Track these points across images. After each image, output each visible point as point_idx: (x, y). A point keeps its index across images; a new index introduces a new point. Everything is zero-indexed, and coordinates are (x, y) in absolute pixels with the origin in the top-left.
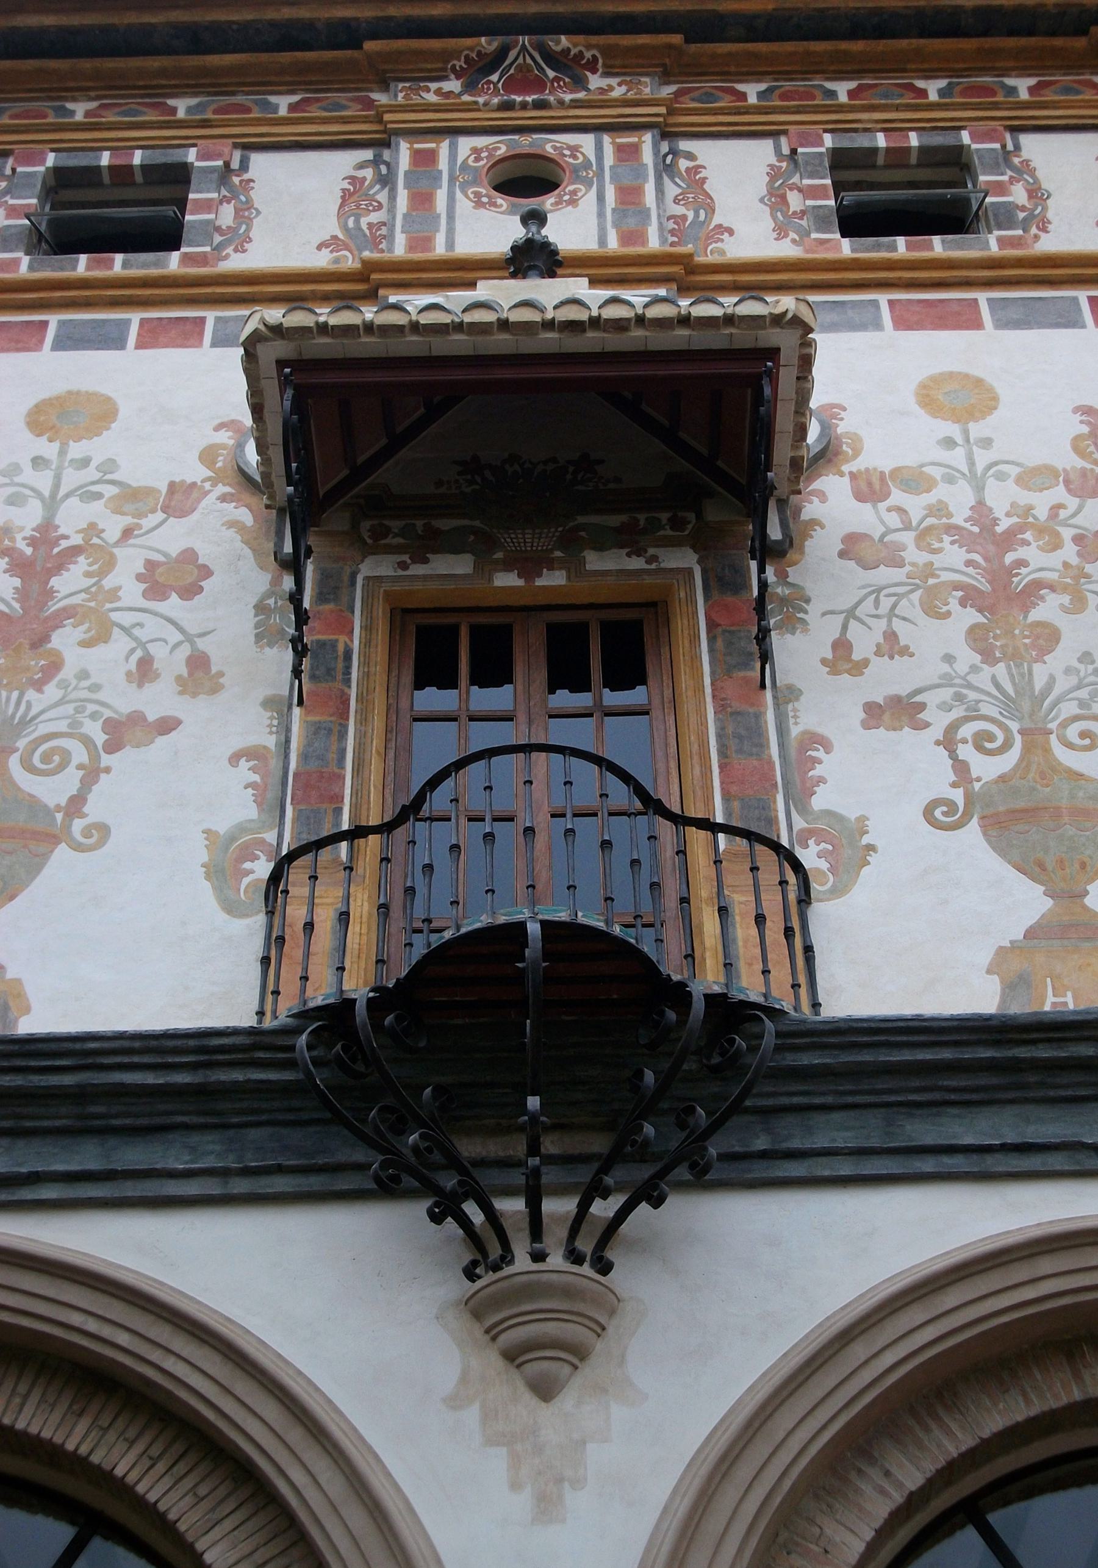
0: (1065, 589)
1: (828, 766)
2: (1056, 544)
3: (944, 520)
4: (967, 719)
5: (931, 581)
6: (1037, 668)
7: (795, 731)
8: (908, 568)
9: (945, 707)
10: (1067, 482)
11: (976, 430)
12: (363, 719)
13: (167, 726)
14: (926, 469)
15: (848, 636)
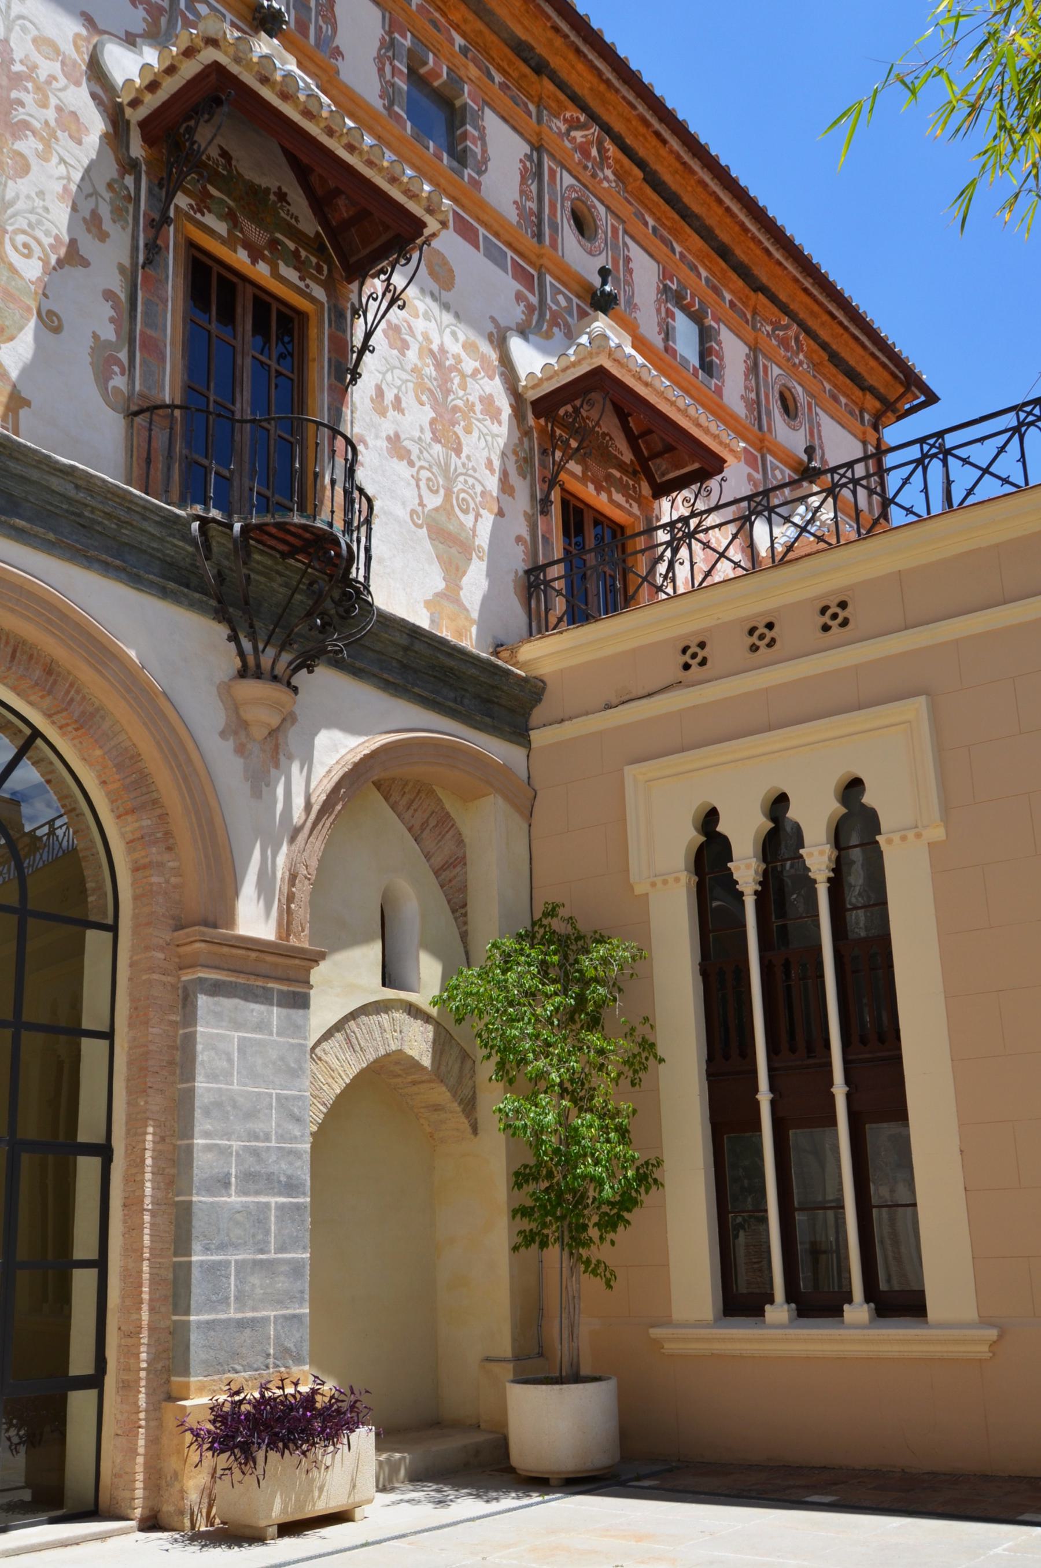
0: (42, 139)
2: (44, 104)
6: (10, 183)
10: (63, 63)
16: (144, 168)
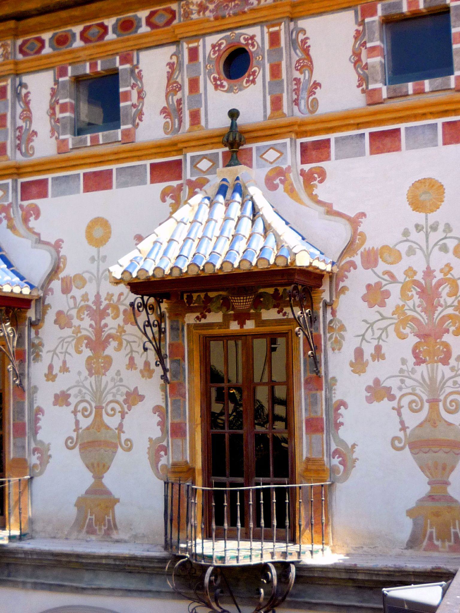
1: (43, 422)
2: (116, 317)
3: (86, 303)
5: (79, 335)
6: (104, 377)
7: (35, 406)
8: (73, 328)
9: (76, 396)
11: (104, 250)
15: (53, 363)
16: (167, 315)
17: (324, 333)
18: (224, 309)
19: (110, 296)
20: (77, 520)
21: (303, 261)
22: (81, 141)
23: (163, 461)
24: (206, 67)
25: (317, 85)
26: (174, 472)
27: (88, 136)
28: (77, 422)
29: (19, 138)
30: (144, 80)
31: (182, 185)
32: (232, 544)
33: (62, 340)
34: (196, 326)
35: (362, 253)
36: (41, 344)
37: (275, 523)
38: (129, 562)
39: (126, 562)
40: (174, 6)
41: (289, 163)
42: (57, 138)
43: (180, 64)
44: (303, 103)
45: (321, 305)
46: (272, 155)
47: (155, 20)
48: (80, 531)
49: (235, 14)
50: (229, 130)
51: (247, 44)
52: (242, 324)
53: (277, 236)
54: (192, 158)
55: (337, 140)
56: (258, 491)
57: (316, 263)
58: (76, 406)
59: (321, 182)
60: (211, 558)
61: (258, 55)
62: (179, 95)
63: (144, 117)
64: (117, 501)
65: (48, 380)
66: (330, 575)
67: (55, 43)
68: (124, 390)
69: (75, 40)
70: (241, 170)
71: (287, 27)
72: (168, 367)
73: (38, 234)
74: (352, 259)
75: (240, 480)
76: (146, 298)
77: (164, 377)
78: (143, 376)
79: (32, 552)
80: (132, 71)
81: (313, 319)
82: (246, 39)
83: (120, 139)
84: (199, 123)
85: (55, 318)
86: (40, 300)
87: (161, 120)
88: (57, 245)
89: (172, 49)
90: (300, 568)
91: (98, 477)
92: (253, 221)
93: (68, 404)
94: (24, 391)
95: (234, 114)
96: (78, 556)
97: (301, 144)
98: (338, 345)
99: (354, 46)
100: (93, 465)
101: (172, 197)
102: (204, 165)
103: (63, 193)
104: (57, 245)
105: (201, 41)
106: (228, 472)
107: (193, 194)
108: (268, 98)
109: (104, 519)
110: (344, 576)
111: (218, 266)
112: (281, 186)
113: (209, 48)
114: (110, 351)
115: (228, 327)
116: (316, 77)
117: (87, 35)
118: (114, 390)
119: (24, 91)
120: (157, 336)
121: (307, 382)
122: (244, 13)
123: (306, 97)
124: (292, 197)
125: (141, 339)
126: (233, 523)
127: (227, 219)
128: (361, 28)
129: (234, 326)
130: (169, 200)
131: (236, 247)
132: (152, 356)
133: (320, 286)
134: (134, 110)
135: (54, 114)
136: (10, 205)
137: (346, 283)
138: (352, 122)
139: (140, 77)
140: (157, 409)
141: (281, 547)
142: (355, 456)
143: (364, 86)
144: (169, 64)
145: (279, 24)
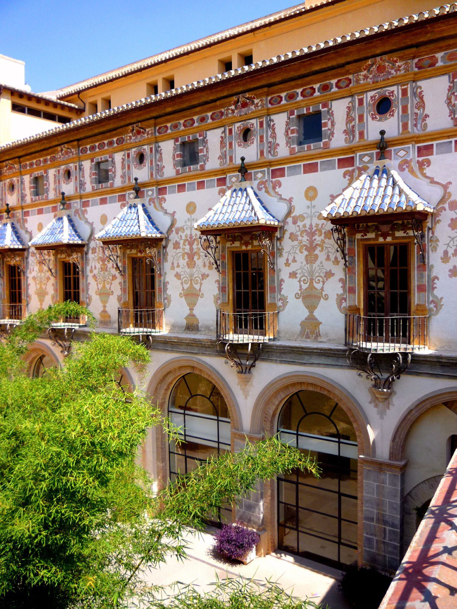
4: (303, 276)
7: (280, 278)
9: (300, 274)
11: (314, 203)
12: (228, 277)
13: (208, 275)
14: (304, 215)
17: (428, 243)
18: (376, 231)
19: (317, 225)
20: (301, 332)
21: (420, 208)
22: (302, 148)
23: (344, 305)
24: (367, 108)
25: (427, 116)
26: (349, 310)
27: (306, 146)
28: (301, 286)
29: (270, 147)
30: (334, 116)
31: (354, 169)
32: (380, 344)
33: (293, 247)
34: (361, 240)
35: (449, 203)
36: (283, 249)
37: (401, 334)
38: (327, 352)
39: (326, 351)
40: (351, 77)
41: (411, 157)
42: (289, 147)
43: (354, 107)
44: (419, 126)
45: (427, 229)
46: (402, 153)
47: (341, 84)
48: (302, 337)
49: (384, 80)
50: (380, 141)
51: (390, 96)
52: (385, 238)
53: (407, 196)
54: (360, 155)
55: (437, 144)
56: (393, 320)
57: (427, 209)
58: (300, 279)
59: (428, 166)
60: (370, 349)
61: (395, 101)
62: (353, 123)
63: (334, 135)
64: (321, 323)
65: (286, 266)
66: (428, 359)
67: (287, 98)
68: (324, 271)
69: (298, 96)
70: (386, 162)
71: (411, 86)
72: (347, 259)
73: (281, 195)
74: (444, 206)
75: (383, 314)
76: (338, 226)
77: (345, 264)
78: (334, 264)
79: (280, 346)
80: (328, 112)
81: (423, 236)
82: (388, 93)
83: (322, 146)
84: (363, 137)
85: (289, 236)
86: (282, 228)
87: (343, 136)
88: (290, 200)
89: (349, 99)
90: (414, 356)
91: (311, 312)
92: (393, 188)
93: (296, 278)
94: (275, 271)
95: (382, 133)
96: (303, 348)
97: (418, 147)
98: (435, 249)
99: (448, 94)
100: (309, 306)
101: (349, 176)
102: (366, 159)
103: (293, 174)
104: (290, 200)
105: (365, 95)
106: (376, 311)
107: (360, 175)
108: (401, 124)
109: (314, 331)
110: (435, 360)
111: (376, 211)
112: (407, 169)
113: (369, 98)
114: (317, 252)
115: (378, 240)
116: (426, 112)
117: (305, 93)
118: (319, 271)
119: (272, 123)
120: (342, 245)
121: (418, 267)
122: (389, 79)
123: (421, 122)
124: (412, 175)
125: (333, 246)
126: (381, 334)
127: (379, 187)
128: (452, 85)
129: (381, 240)
130: (347, 177)
131: (385, 201)
132: (339, 255)
133: (426, 219)
134: (329, 132)
135: (288, 134)
136: (266, 181)
137: (440, 218)
138: (446, 135)
139: (332, 114)
140: (341, 280)
141: (404, 346)
142: (442, 303)
143: (453, 116)
144: (347, 107)
145: (407, 84)
